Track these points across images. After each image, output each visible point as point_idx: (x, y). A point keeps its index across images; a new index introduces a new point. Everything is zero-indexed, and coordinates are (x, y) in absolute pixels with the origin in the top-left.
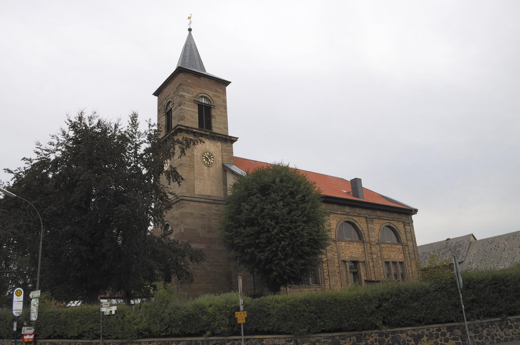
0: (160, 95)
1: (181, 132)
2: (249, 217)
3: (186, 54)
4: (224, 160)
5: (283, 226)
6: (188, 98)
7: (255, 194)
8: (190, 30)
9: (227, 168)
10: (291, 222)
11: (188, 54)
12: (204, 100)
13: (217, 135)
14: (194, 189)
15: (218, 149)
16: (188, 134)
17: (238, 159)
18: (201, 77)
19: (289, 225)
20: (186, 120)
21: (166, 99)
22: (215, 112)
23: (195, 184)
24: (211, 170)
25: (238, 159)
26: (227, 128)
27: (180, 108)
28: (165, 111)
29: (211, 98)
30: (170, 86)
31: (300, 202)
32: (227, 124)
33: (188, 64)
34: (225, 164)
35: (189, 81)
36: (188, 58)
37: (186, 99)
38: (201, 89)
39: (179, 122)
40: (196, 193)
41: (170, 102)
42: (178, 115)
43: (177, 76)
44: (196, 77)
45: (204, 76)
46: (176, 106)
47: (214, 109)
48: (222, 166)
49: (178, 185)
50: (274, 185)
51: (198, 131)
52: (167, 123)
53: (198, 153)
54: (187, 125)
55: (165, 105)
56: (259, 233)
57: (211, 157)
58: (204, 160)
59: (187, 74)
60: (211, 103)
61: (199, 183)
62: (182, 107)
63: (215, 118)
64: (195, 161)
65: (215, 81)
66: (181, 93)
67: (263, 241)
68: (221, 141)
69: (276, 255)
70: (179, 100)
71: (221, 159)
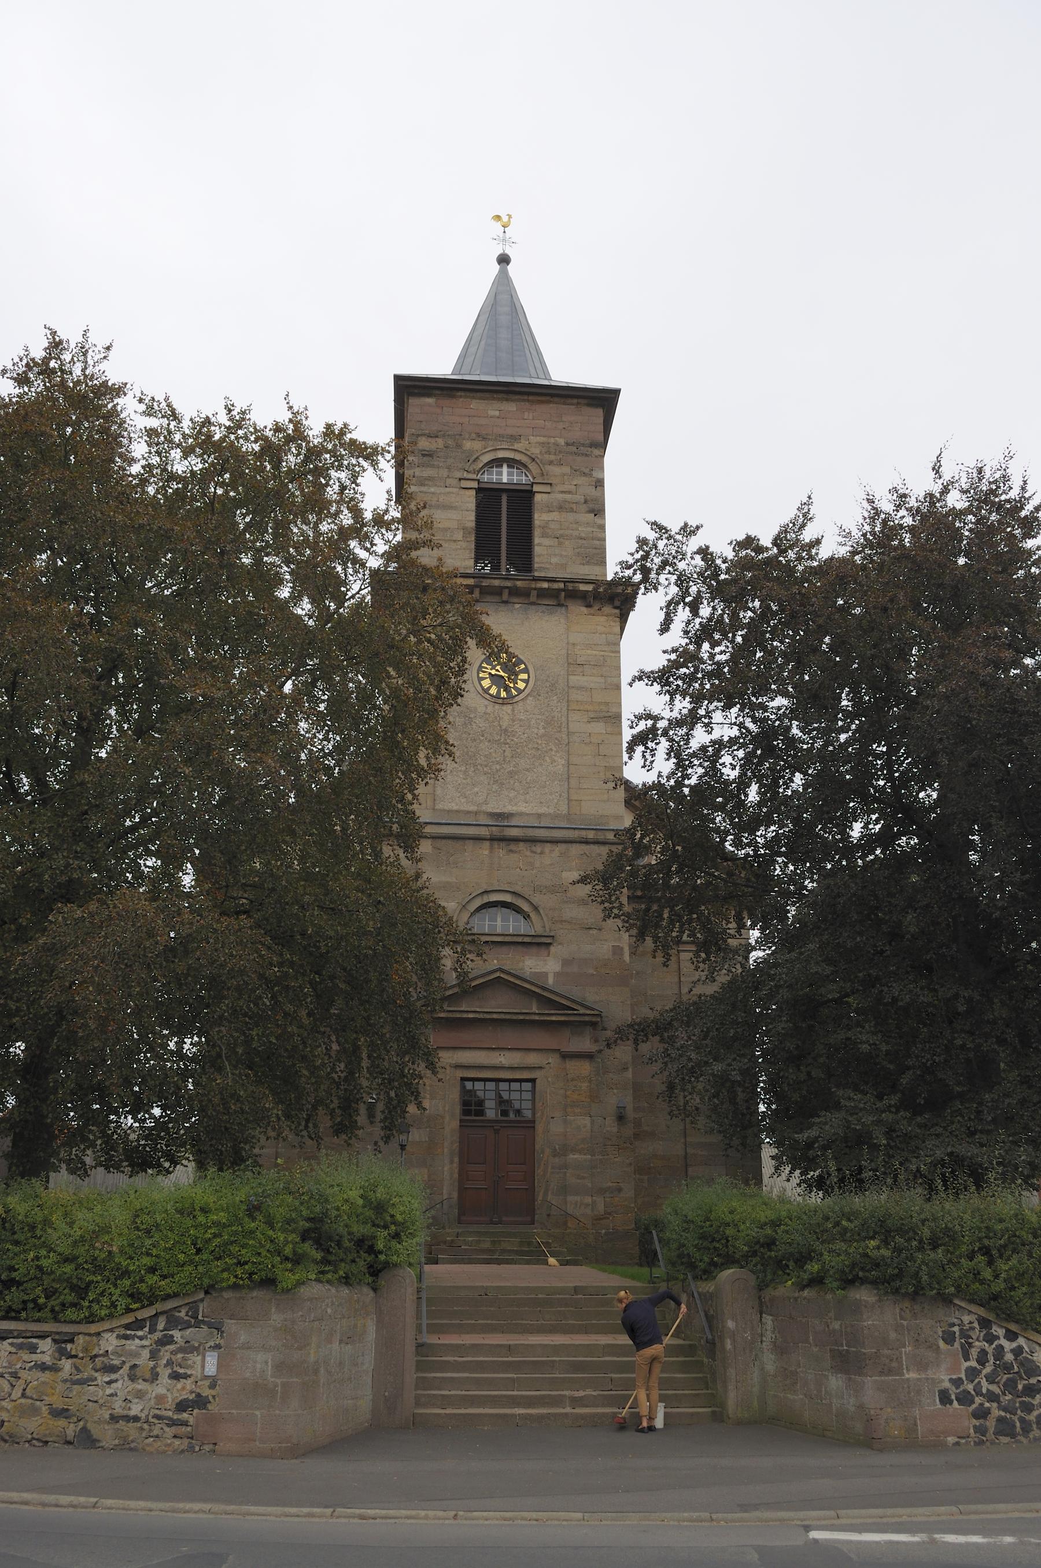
8: (504, 260)
12: (509, 474)
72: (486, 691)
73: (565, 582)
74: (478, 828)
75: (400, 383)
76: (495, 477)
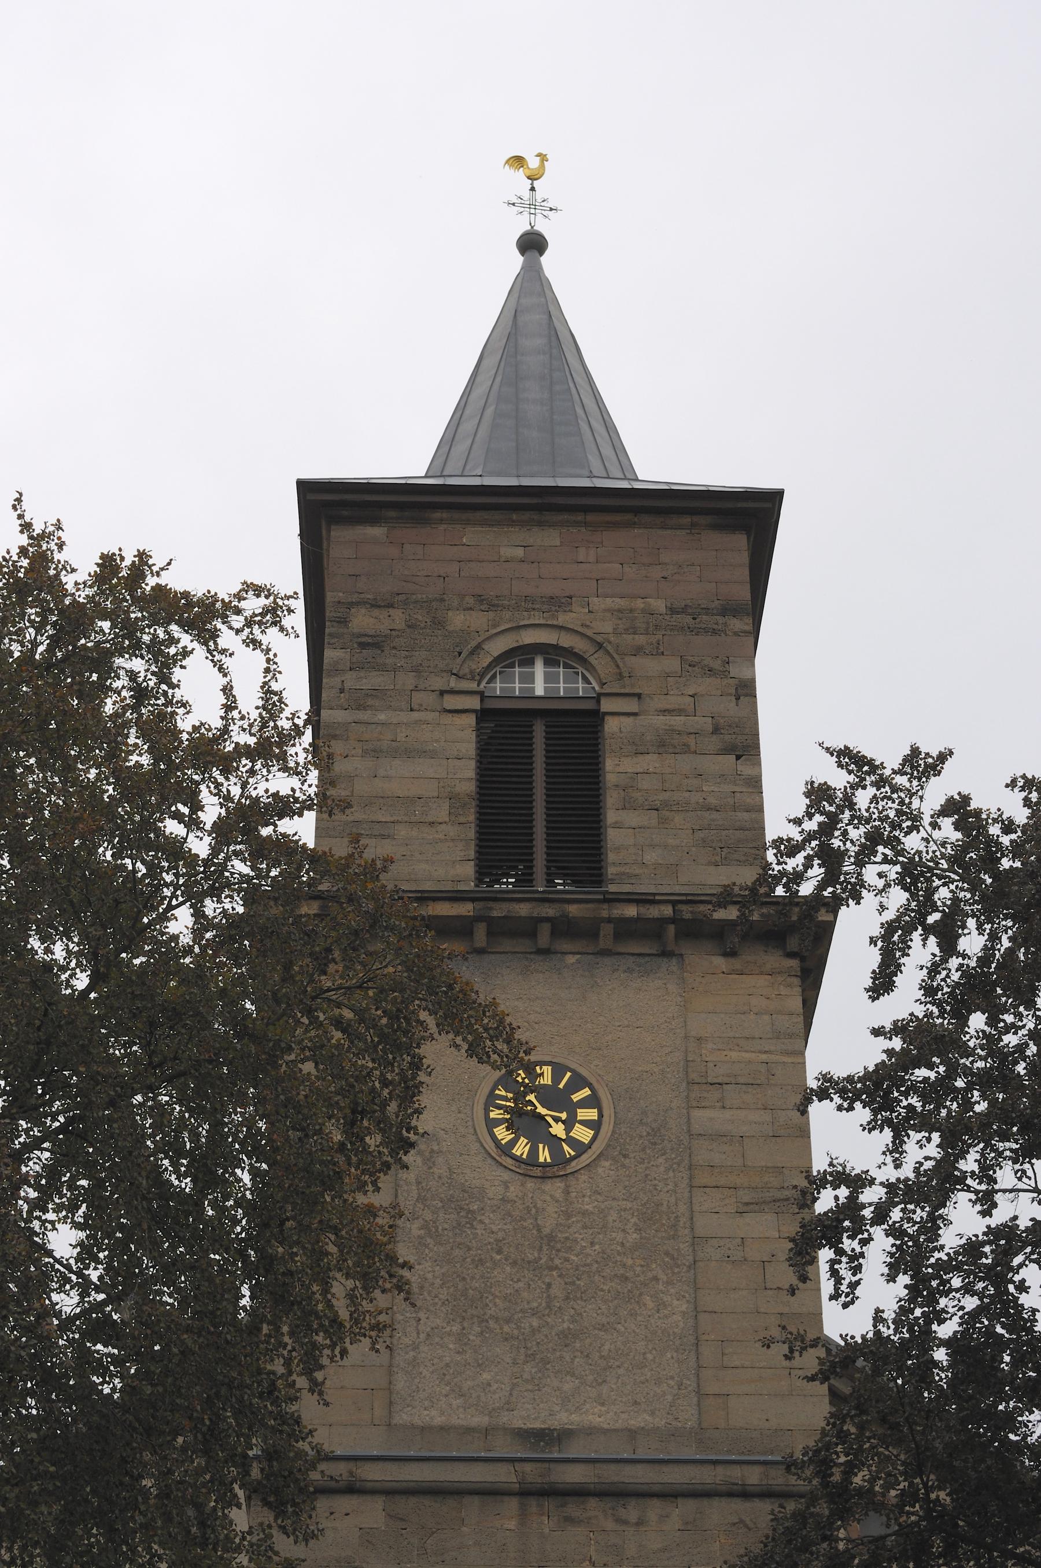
12: (548, 678)
57: (576, 1097)
73: (674, 903)
74: (491, 1466)
75: (311, 497)
76: (517, 685)
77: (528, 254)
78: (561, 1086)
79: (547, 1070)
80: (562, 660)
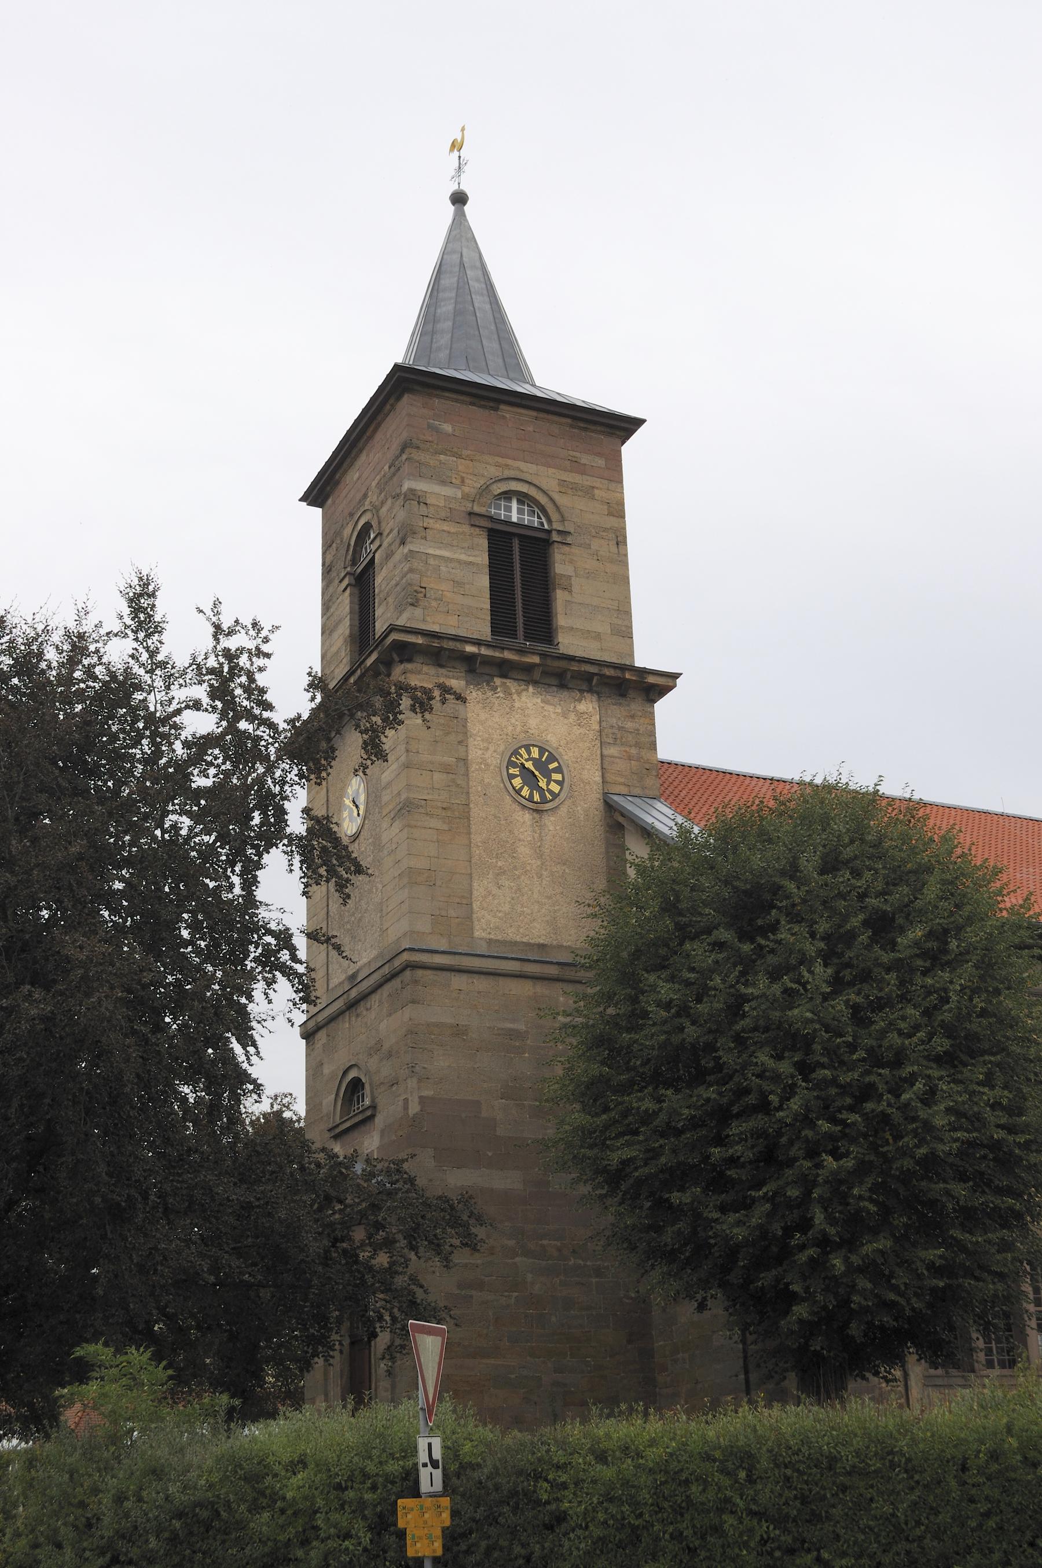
0: (330, 501)
1: (410, 660)
2: (676, 1039)
3: (439, 311)
4: (610, 777)
5: (834, 1082)
6: (442, 504)
7: (709, 933)
8: (459, 199)
9: (623, 815)
10: (875, 1059)
11: (447, 308)
12: (520, 512)
13: (575, 667)
14: (469, 917)
15: (582, 730)
16: (441, 666)
17: (691, 774)
18: (502, 407)
19: (868, 1073)
20: (434, 604)
21: (351, 515)
22: (571, 562)
23: (475, 893)
24: (551, 828)
25: (691, 774)
26: (627, 634)
27: (406, 551)
28: (349, 569)
29: (551, 499)
30: (368, 455)
31: (919, 962)
32: (628, 613)
33: (448, 352)
34: (615, 798)
35: (447, 428)
36: (450, 323)
37: (431, 509)
38: (500, 460)
39: (401, 613)
40: (477, 934)
41: (367, 526)
42: (397, 585)
43: (393, 406)
44: (480, 406)
45: (518, 401)
46: (390, 545)
47: (566, 549)
48: (600, 805)
49: (337, 894)
50: (791, 886)
51: (484, 651)
52: (357, 623)
53: (490, 752)
54: (436, 628)
55: (349, 544)
56: (724, 1115)
57: (552, 766)
58: (517, 782)
59: (438, 396)
60: (549, 521)
61: (495, 890)
62: (415, 545)
63: (568, 589)
64: (475, 787)
65: (569, 421)
66: (407, 485)
67: (739, 1154)
68: (598, 693)
69: (805, 1225)
70: (401, 515)
71: (598, 774)
72: (518, 792)
76: (503, 512)
77: (456, 205)
78: (543, 759)
79: (536, 750)
80: (526, 501)
